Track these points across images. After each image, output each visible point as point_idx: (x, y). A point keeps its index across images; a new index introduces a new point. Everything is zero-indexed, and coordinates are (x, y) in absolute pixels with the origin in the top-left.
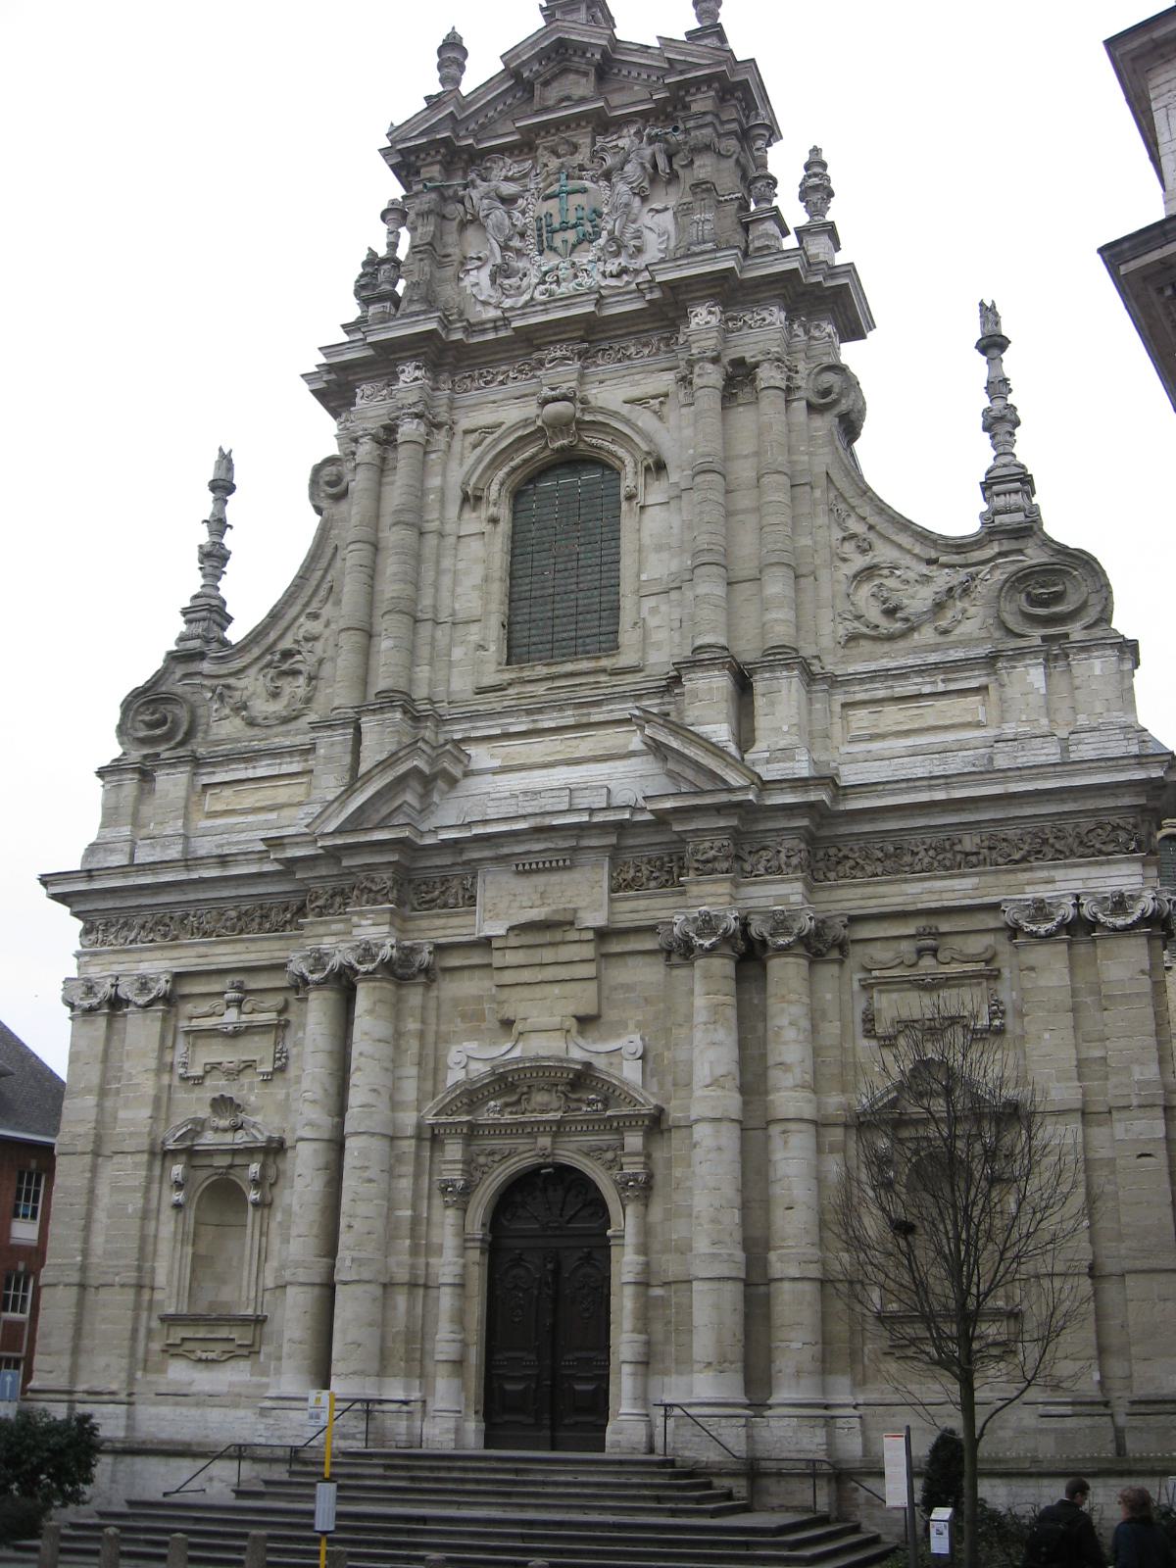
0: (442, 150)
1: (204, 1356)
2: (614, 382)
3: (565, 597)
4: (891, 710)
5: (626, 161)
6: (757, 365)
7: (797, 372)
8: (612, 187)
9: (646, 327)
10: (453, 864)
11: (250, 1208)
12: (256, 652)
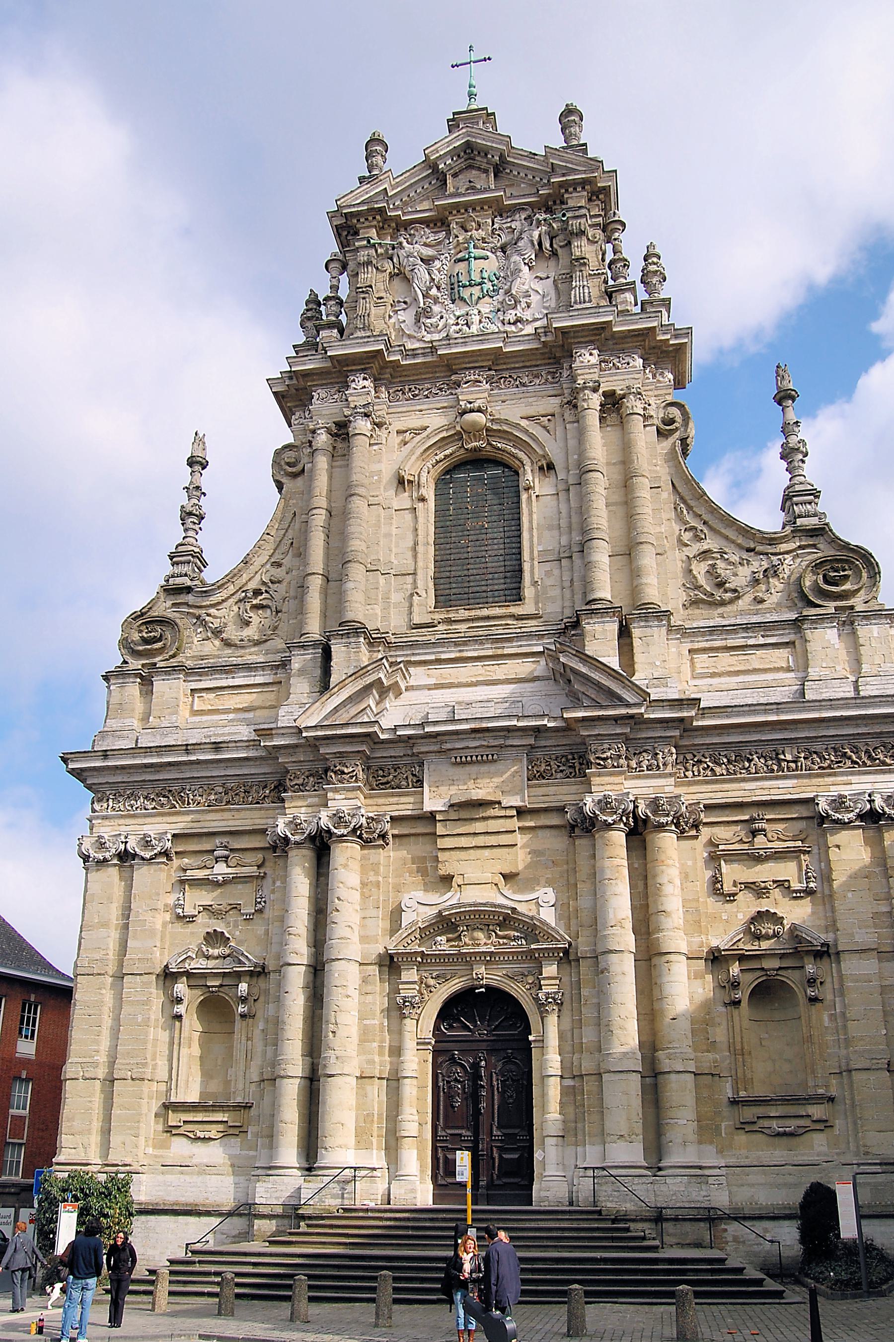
0: (378, 217)
2: (514, 402)
3: (478, 560)
4: (724, 657)
5: (519, 238)
6: (624, 396)
7: (649, 405)
8: (507, 258)
9: (538, 363)
11: (238, 1018)
12: (231, 589)
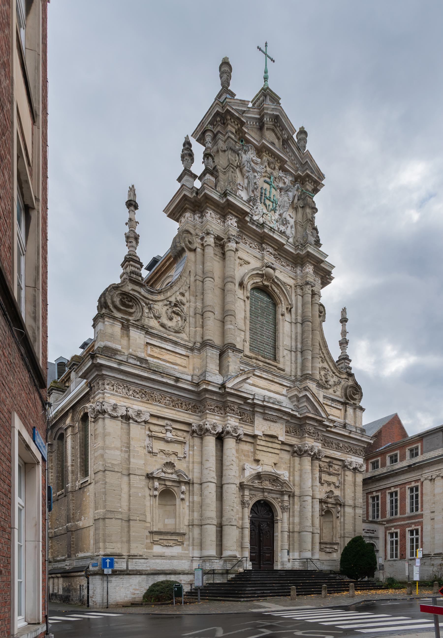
1: (167, 544)
10: (249, 410)
